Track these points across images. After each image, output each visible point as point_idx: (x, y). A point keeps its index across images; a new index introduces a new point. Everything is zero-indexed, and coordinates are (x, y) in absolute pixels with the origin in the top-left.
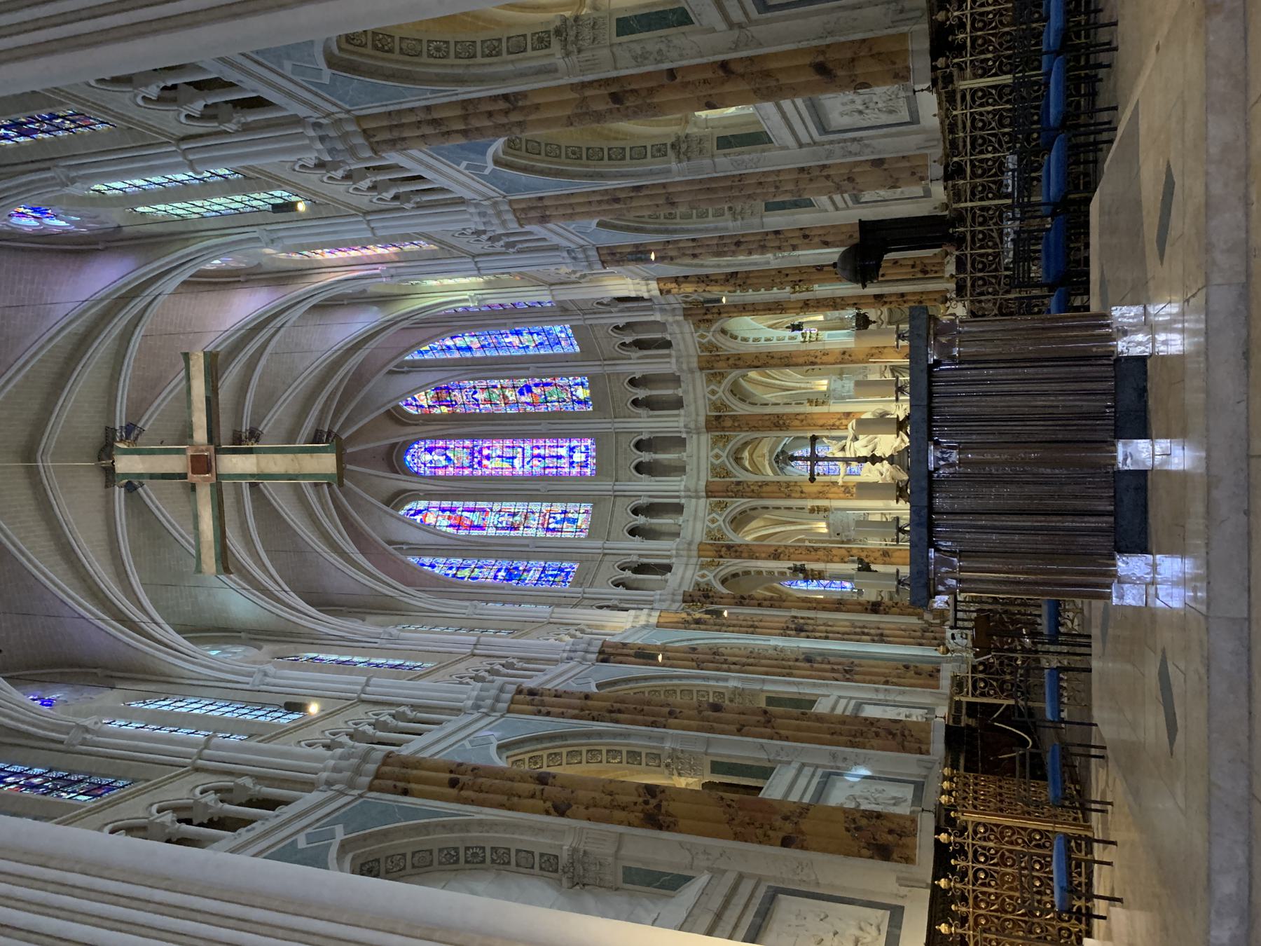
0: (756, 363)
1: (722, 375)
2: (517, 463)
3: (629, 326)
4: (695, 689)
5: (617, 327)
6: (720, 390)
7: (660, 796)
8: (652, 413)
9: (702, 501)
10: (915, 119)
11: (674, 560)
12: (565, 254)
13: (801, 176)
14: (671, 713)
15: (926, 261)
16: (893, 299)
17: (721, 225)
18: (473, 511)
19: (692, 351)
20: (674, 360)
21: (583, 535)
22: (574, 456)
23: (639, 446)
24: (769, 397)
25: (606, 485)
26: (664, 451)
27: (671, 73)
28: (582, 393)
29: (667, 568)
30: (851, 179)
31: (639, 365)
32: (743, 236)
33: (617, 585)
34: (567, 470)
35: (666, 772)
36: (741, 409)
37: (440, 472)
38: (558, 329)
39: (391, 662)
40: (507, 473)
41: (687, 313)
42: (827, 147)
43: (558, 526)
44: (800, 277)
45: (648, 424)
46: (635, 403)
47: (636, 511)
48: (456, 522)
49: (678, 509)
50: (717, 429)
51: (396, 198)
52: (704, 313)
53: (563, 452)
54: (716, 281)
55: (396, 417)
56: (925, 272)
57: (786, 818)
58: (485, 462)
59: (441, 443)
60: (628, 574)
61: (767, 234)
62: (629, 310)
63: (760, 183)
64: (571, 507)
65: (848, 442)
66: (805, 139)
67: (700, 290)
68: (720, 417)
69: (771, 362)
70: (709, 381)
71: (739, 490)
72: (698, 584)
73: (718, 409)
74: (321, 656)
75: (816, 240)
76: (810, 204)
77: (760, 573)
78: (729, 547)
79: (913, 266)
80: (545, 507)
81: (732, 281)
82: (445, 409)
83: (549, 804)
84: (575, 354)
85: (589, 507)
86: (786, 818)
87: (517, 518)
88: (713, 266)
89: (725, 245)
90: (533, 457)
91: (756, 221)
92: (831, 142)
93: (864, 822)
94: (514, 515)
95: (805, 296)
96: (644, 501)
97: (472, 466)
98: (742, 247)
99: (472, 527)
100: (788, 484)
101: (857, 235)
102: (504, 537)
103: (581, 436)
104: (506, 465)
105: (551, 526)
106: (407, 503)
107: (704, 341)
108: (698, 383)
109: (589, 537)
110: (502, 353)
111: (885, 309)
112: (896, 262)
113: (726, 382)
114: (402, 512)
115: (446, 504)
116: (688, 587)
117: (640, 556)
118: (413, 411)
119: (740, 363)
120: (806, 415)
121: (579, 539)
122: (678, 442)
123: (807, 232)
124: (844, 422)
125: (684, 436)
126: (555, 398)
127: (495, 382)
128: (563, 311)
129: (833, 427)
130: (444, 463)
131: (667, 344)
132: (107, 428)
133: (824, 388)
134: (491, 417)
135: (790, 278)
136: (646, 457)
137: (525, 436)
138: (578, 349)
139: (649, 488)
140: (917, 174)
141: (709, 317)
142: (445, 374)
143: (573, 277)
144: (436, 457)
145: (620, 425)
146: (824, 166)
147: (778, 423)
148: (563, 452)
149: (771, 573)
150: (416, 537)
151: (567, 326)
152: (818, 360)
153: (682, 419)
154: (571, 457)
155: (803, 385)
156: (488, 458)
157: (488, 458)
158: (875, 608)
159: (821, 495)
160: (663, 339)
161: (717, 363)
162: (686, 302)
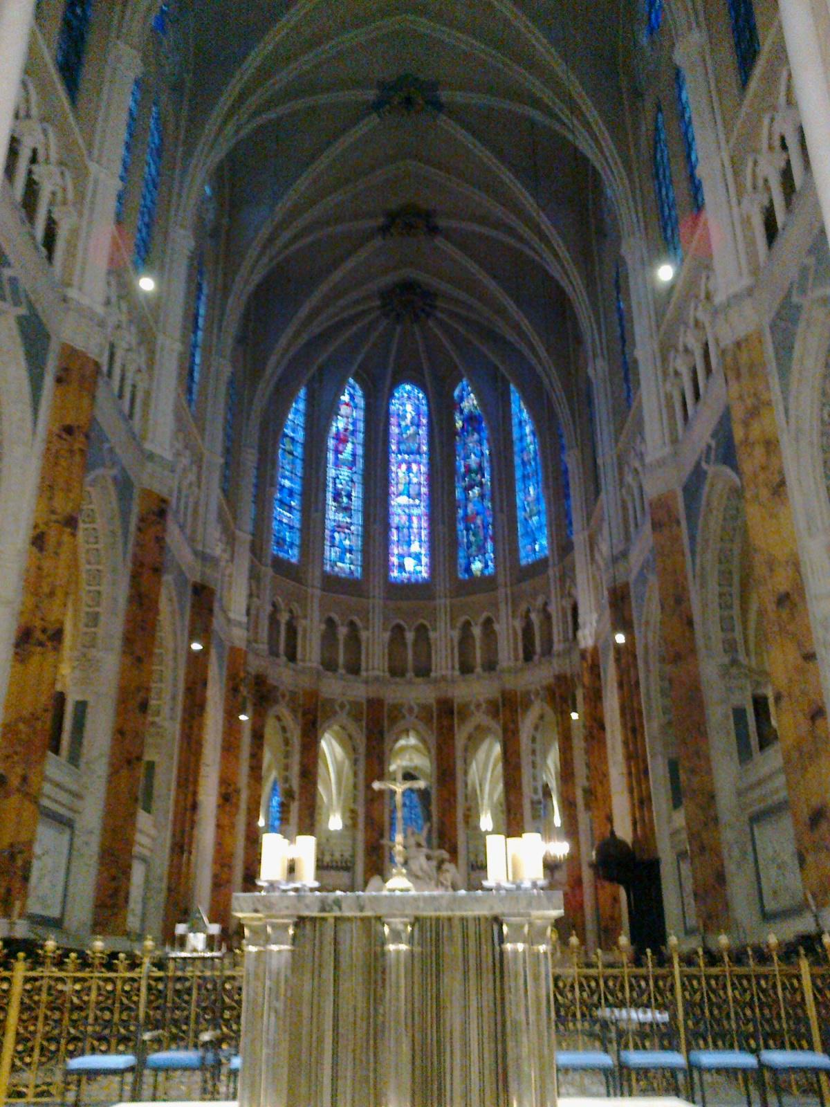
1: (495, 715)
2: (403, 500)
3: (548, 617)
4: (163, 685)
5: (546, 604)
7: (49, 644)
8: (456, 643)
10: (767, 917)
12: (621, 547)
14: (140, 659)
18: (354, 455)
20: (512, 664)
21: (328, 568)
22: (411, 560)
24: (474, 767)
27: (810, 657)
28: (477, 566)
33: (274, 605)
34: (396, 551)
35: (76, 653)
37: (393, 420)
38: (544, 542)
39: (196, 368)
40: (393, 489)
41: (561, 679)
43: (337, 542)
46: (467, 626)
47: (352, 624)
48: (342, 436)
49: (354, 669)
51: (677, 374)
52: (560, 695)
53: (415, 548)
57: (25, 779)
58: (404, 467)
59: (424, 421)
61: (645, 760)
62: (565, 616)
64: (358, 557)
65: (425, 850)
72: (275, 688)
74: (203, 298)
76: (677, 802)
79: (612, 918)
82: (459, 424)
83: (42, 527)
84: (518, 560)
85: (358, 573)
86: (25, 779)
87: (345, 500)
90: (410, 517)
93: (19, 863)
94: (349, 496)
96: (364, 635)
97: (400, 452)
101: (645, 857)
102: (325, 486)
103: (432, 568)
104: (401, 487)
105: (336, 535)
106: (361, 387)
109: (324, 574)
110: (519, 485)
112: (616, 900)
114: (351, 381)
115: (361, 426)
116: (271, 681)
117: (305, 630)
118: (456, 393)
121: (323, 564)
122: (424, 671)
124: (447, 846)
125: (433, 675)
126: (472, 539)
127: (487, 476)
128: (563, 547)
130: (403, 424)
134: (453, 471)
136: (410, 636)
138: (523, 562)
139: (375, 641)
143: (597, 556)
144: (409, 416)
146: (716, 820)
148: (415, 548)
151: (547, 552)
153: (449, 673)
154: (410, 555)
155: (486, 801)
156: (409, 469)
157: (409, 469)
160: (534, 653)
161: (507, 710)
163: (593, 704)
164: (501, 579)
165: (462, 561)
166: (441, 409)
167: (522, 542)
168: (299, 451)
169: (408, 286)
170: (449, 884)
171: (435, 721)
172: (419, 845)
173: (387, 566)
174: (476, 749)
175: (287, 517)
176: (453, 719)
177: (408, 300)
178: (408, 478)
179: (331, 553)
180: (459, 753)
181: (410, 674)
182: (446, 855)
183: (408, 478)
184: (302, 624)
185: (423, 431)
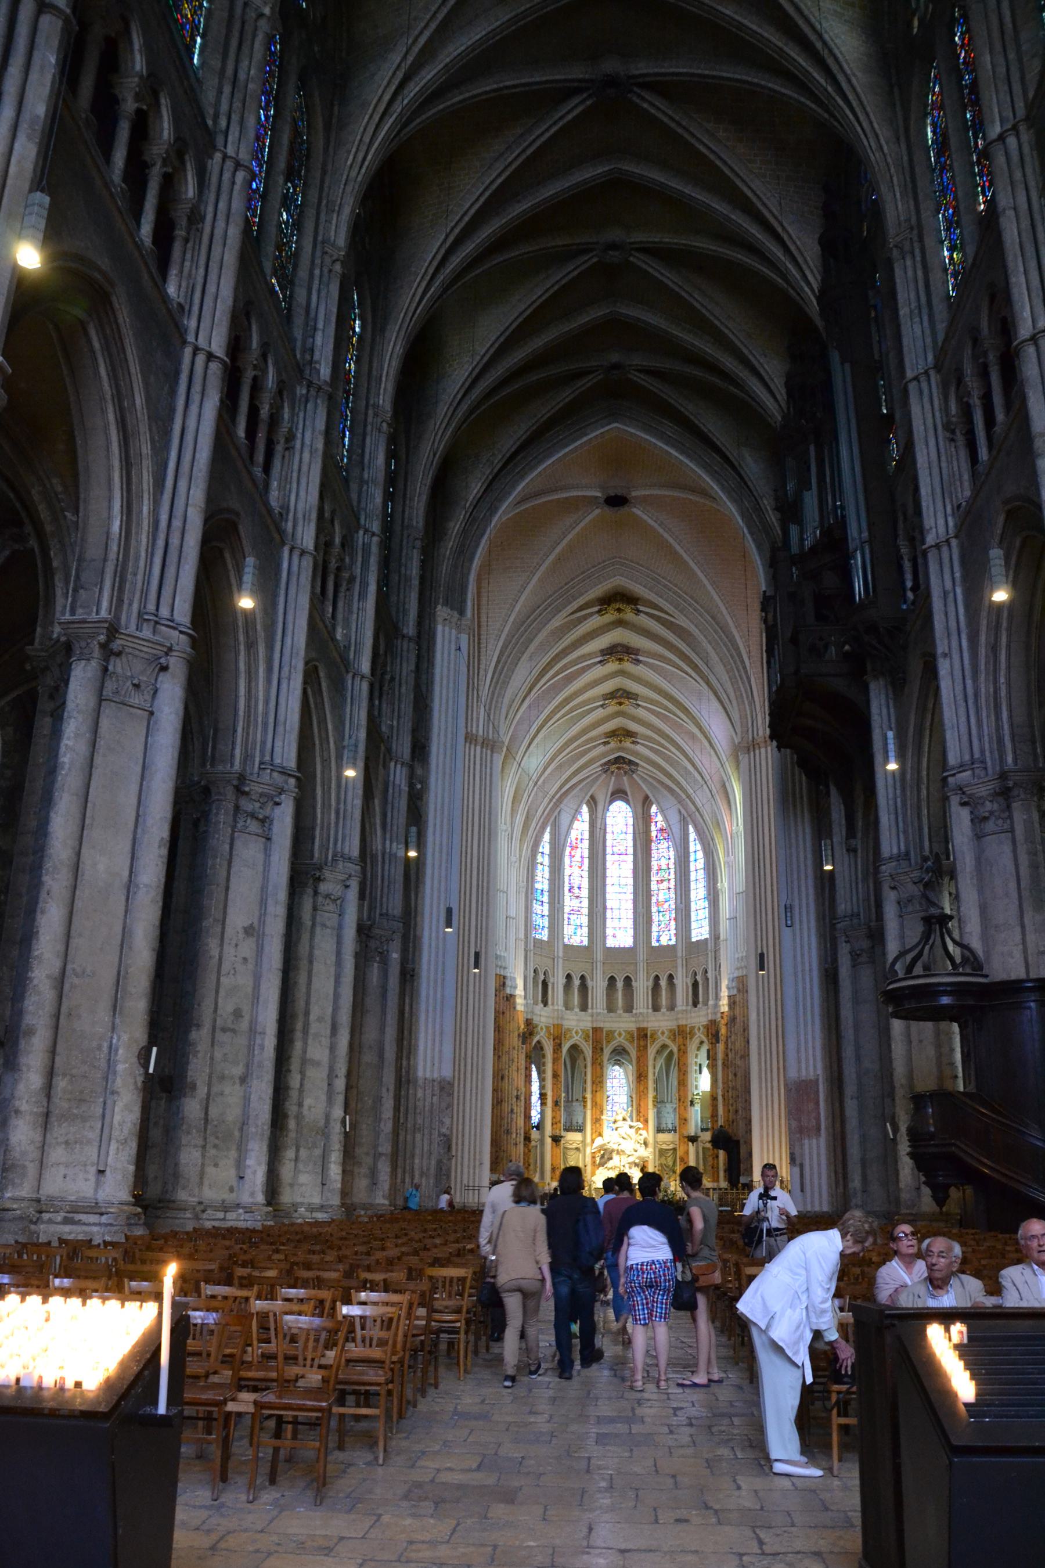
1: (674, 1040)
2: (616, 889)
9: (589, 1025)
11: (550, 1007)
22: (620, 933)
23: (628, 980)
25: (599, 956)
26: (624, 995)
29: (545, 1003)
31: (682, 983)
36: (652, 1051)
37: (608, 830)
40: (608, 881)
41: (713, 1023)
45: (642, 986)
46: (657, 978)
47: (583, 978)
49: (584, 1007)
52: (713, 1033)
55: (646, 802)
59: (631, 830)
60: (542, 977)
64: (585, 930)
65: (629, 1122)
70: (671, 1031)
71: (598, 1049)
73: (652, 1036)
77: (544, 1064)
78: (560, 1045)
80: (585, 911)
82: (654, 834)
85: (586, 943)
96: (589, 983)
99: (572, 856)
100: (601, 1082)
103: (635, 937)
108: (669, 1023)
109: (565, 946)
110: (693, 885)
113: (669, 1042)
116: (536, 1020)
118: (654, 809)
120: (646, 1095)
122: (629, 1008)
127: (672, 876)
129: (639, 1112)
131: (695, 1004)
132: (638, 650)
136: (620, 984)
137: (635, 893)
139: (598, 986)
142: (678, 840)
145: (642, 967)
149: (544, 1072)
150: (565, 819)
158: (527, 1139)
159: (595, 1104)
164: (679, 947)
165: (654, 935)
166: (642, 821)
167: (694, 925)
168: (546, 861)
169: (619, 760)
173: (605, 937)
175: (541, 910)
177: (621, 764)
178: (620, 873)
179: (568, 930)
181: (620, 1011)
183: (620, 873)
184: (551, 980)
185: (630, 837)
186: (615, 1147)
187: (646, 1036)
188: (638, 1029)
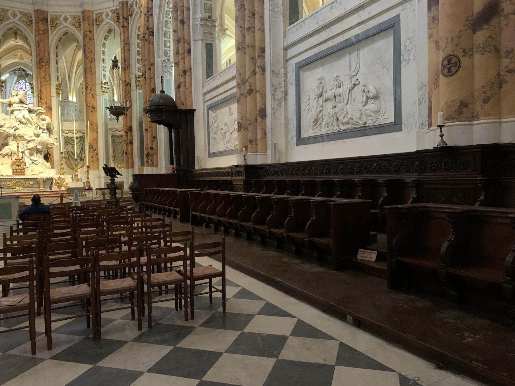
0: (87, 49)
1: (78, 27)
6: (67, 24)
10: (301, 141)
13: (257, 50)
15: (154, 156)
16: (129, 137)
17: (198, 9)
19: (97, 7)
30: (251, 91)
32: (189, 26)
36: (53, 37)
42: (282, 71)
44: (148, 75)
50: (37, 18)
54: (148, 21)
56: (147, 156)
61: (189, 44)
63: (254, 15)
66: (291, 52)
67: (142, 9)
68: (47, 22)
69: (88, 61)
75: (182, 80)
79: (152, 148)
81: (147, 32)
88: (159, 18)
89: (182, 12)
91: (199, 36)
92: (286, 75)
95: (133, 84)
98: (179, 25)
101: (183, 108)
107: (104, 16)
108: (72, 9)
111: (123, 133)
113: (73, 30)
119: (87, 40)
123: (188, 73)
124: (44, 106)
133: (70, 99)
135: (147, 71)
140: (250, 143)
141: (121, 19)
146: (263, 69)
147: (42, 62)
152: (89, 91)
155: (72, 86)
162: (132, 3)
163: (147, 18)
170: (46, 128)
171: (34, 25)
172: (21, 102)
174: (65, 50)
176: (47, 25)
180: (52, 50)
182: (44, 111)
186: (11, 131)
187: (46, 20)
188: (36, 11)
